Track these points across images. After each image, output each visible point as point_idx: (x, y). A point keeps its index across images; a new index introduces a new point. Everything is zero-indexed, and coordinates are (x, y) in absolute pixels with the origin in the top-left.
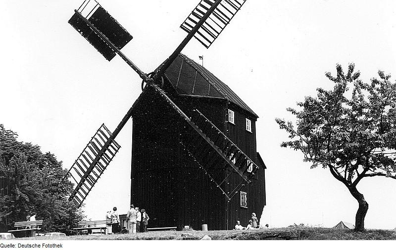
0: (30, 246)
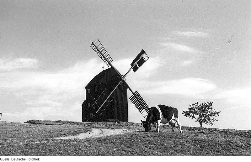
0: (19, 160)
